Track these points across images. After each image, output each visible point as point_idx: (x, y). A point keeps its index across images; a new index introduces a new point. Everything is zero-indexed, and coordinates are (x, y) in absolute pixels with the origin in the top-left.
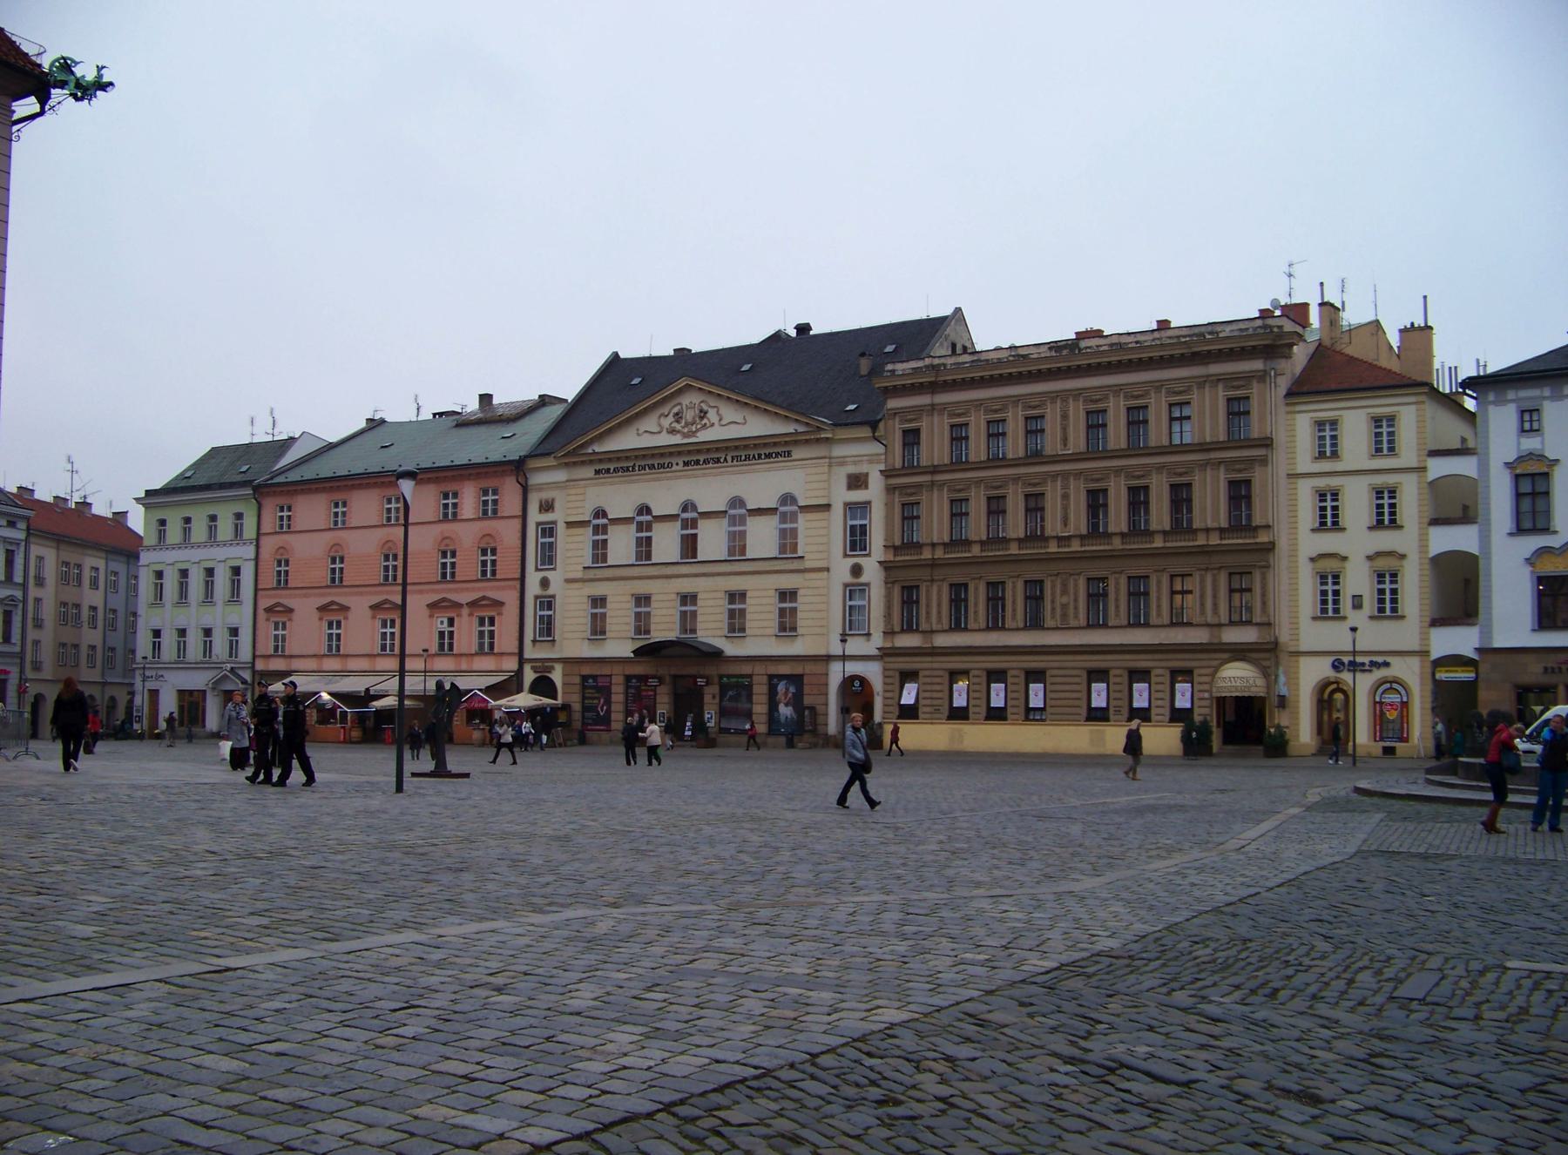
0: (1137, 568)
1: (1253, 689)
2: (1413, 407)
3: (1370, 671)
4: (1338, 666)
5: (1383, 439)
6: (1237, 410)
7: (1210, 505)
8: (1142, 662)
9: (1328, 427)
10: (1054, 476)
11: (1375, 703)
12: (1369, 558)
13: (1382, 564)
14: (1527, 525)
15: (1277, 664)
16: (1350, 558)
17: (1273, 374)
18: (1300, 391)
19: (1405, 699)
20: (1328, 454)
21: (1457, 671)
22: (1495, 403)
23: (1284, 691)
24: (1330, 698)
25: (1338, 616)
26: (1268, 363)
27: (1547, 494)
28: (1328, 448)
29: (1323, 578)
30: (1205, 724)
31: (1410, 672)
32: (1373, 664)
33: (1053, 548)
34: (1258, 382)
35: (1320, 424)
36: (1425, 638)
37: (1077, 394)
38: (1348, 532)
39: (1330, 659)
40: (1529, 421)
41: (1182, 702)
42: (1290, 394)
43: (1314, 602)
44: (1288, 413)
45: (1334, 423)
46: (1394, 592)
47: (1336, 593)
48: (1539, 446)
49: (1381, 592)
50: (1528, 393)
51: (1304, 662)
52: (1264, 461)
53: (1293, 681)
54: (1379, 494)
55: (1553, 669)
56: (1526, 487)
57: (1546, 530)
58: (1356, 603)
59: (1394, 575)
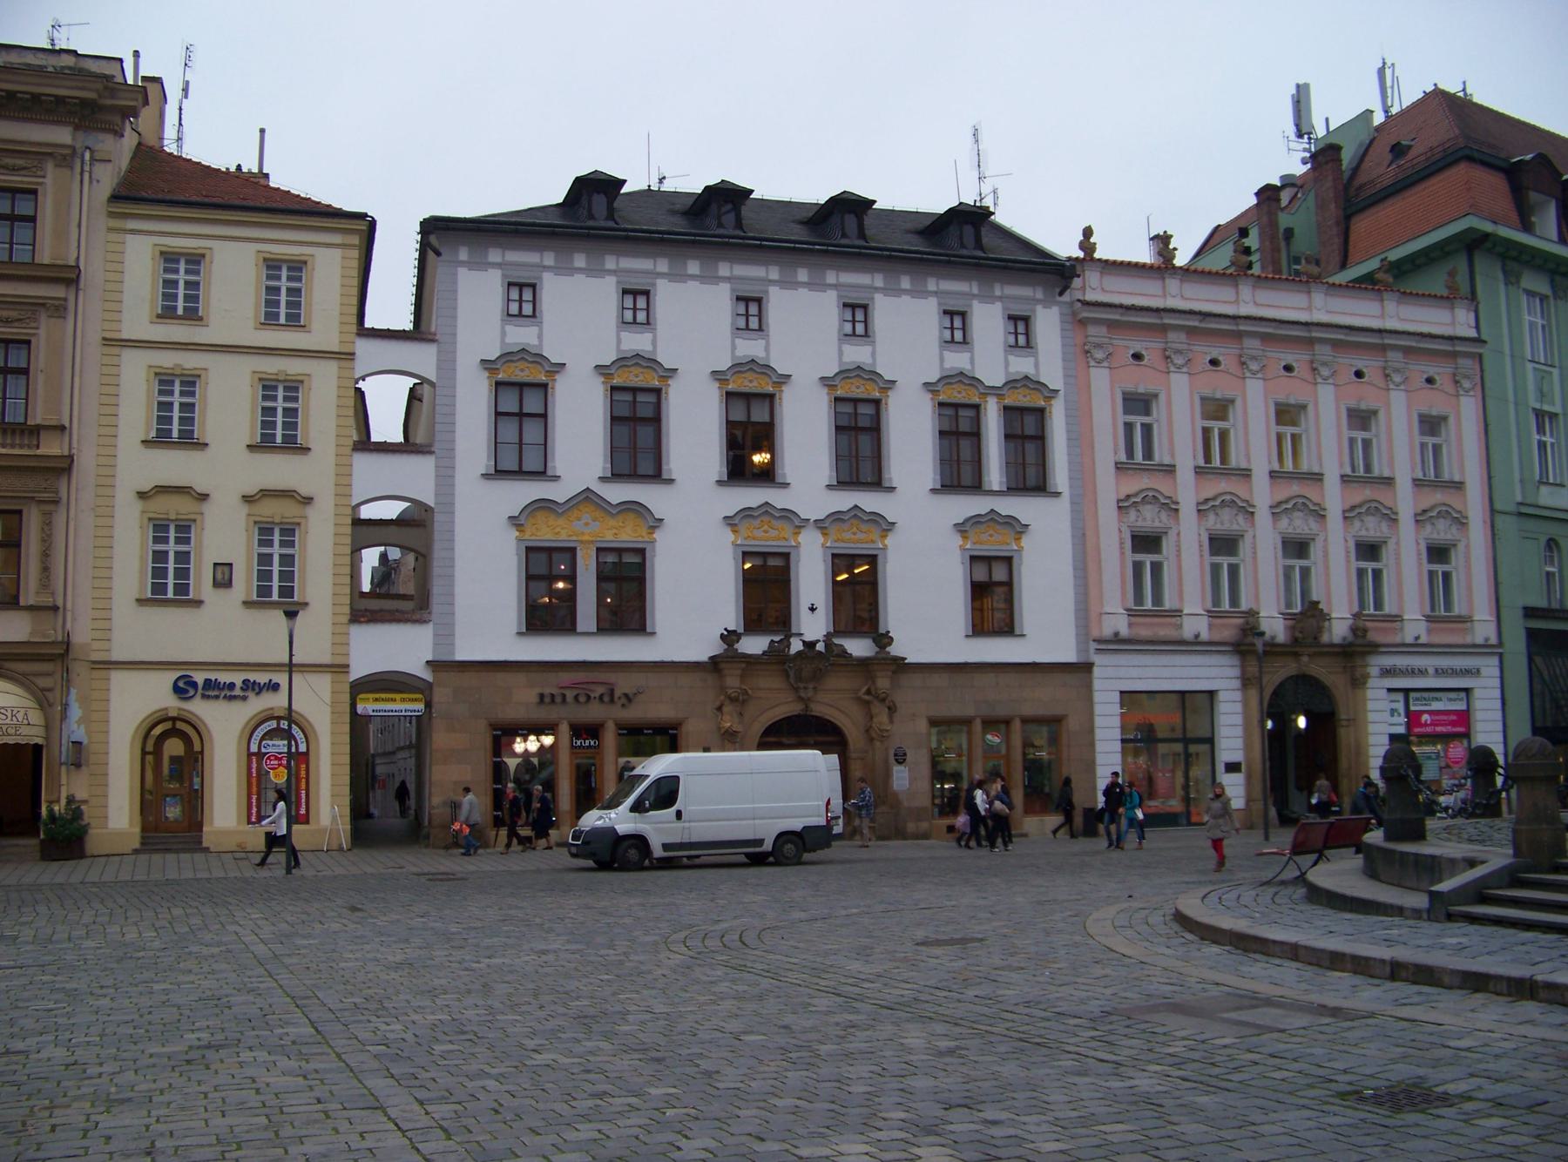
1: (25, 730)
2: (338, 253)
3: (244, 698)
4: (183, 689)
9: (182, 266)
11: (250, 755)
12: (248, 499)
13: (272, 510)
15: (67, 683)
16: (214, 496)
17: (87, 156)
19: (303, 748)
20: (180, 312)
21: (393, 700)
22: (471, 265)
23: (80, 733)
25: (184, 598)
26: (80, 135)
27: (544, 416)
29: (160, 529)
32: (248, 685)
34: (56, 166)
35: (169, 259)
36: (341, 643)
38: (209, 451)
39: (172, 676)
42: (115, 198)
43: (142, 572)
44: (110, 230)
45: (195, 260)
46: (287, 560)
47: (183, 557)
48: (535, 342)
49: (265, 559)
50: (523, 258)
51: (118, 678)
52: (58, 309)
53: (99, 716)
54: (268, 387)
55: (553, 696)
56: (510, 403)
57: (542, 474)
58: (219, 576)
59: (289, 532)
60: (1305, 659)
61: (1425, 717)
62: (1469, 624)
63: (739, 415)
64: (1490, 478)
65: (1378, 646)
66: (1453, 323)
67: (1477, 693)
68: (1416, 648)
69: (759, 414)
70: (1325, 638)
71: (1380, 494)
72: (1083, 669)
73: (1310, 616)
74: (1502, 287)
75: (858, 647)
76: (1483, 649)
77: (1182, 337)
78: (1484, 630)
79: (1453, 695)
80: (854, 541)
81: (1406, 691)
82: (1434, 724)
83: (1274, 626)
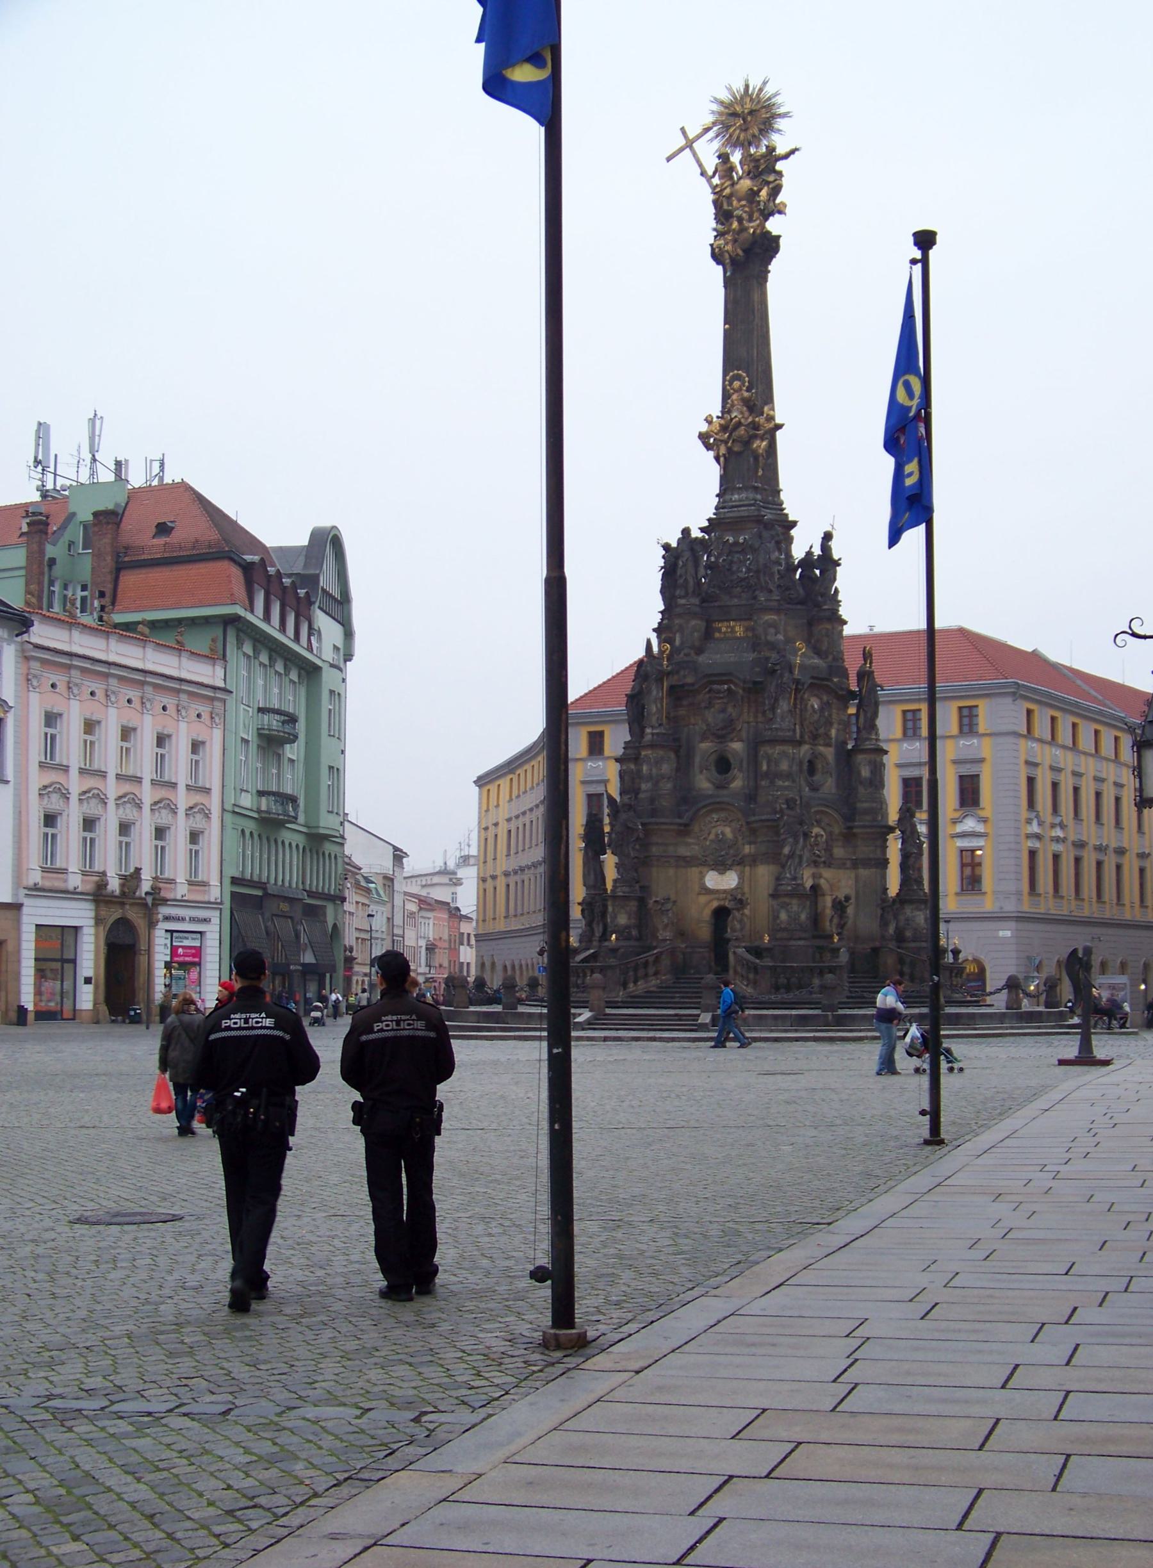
60: (127, 907)
61: (180, 951)
62: (207, 888)
64: (223, 786)
65: (168, 900)
66: (213, 676)
67: (208, 935)
68: (183, 903)
70: (137, 894)
72: (17, 907)
73: (132, 879)
77: (78, 673)
78: (214, 893)
79: (194, 936)
81: (172, 932)
82: (185, 955)
83: (114, 885)
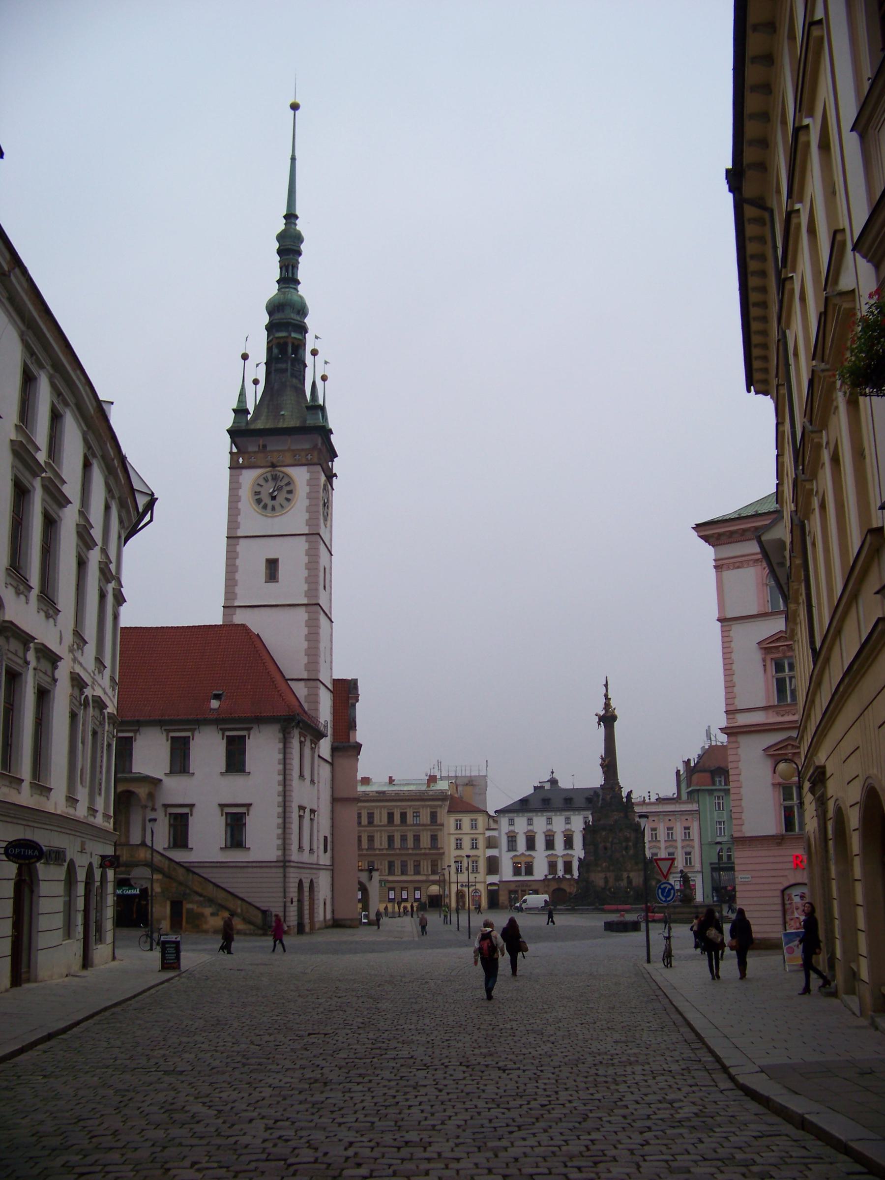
0: (404, 858)
4: (462, 886)
5: (474, 826)
6: (434, 816)
7: (426, 841)
8: (405, 885)
10: (377, 831)
14: (510, 848)
18: (450, 812)
24: (460, 895)
27: (515, 841)
28: (459, 827)
30: (425, 902)
31: (481, 887)
33: (377, 852)
35: (457, 820)
37: (384, 807)
40: (511, 822)
41: (418, 896)
42: (448, 812)
45: (460, 820)
50: (511, 815)
52: (441, 830)
56: (510, 839)
57: (516, 850)
59: (476, 862)
63: (548, 838)
69: (552, 838)
71: (673, 843)
74: (707, 797)
75: (568, 876)
76: (698, 872)
80: (568, 859)
